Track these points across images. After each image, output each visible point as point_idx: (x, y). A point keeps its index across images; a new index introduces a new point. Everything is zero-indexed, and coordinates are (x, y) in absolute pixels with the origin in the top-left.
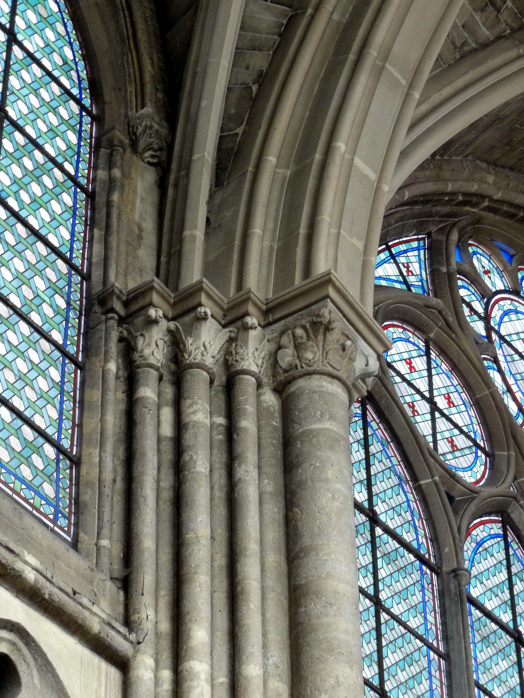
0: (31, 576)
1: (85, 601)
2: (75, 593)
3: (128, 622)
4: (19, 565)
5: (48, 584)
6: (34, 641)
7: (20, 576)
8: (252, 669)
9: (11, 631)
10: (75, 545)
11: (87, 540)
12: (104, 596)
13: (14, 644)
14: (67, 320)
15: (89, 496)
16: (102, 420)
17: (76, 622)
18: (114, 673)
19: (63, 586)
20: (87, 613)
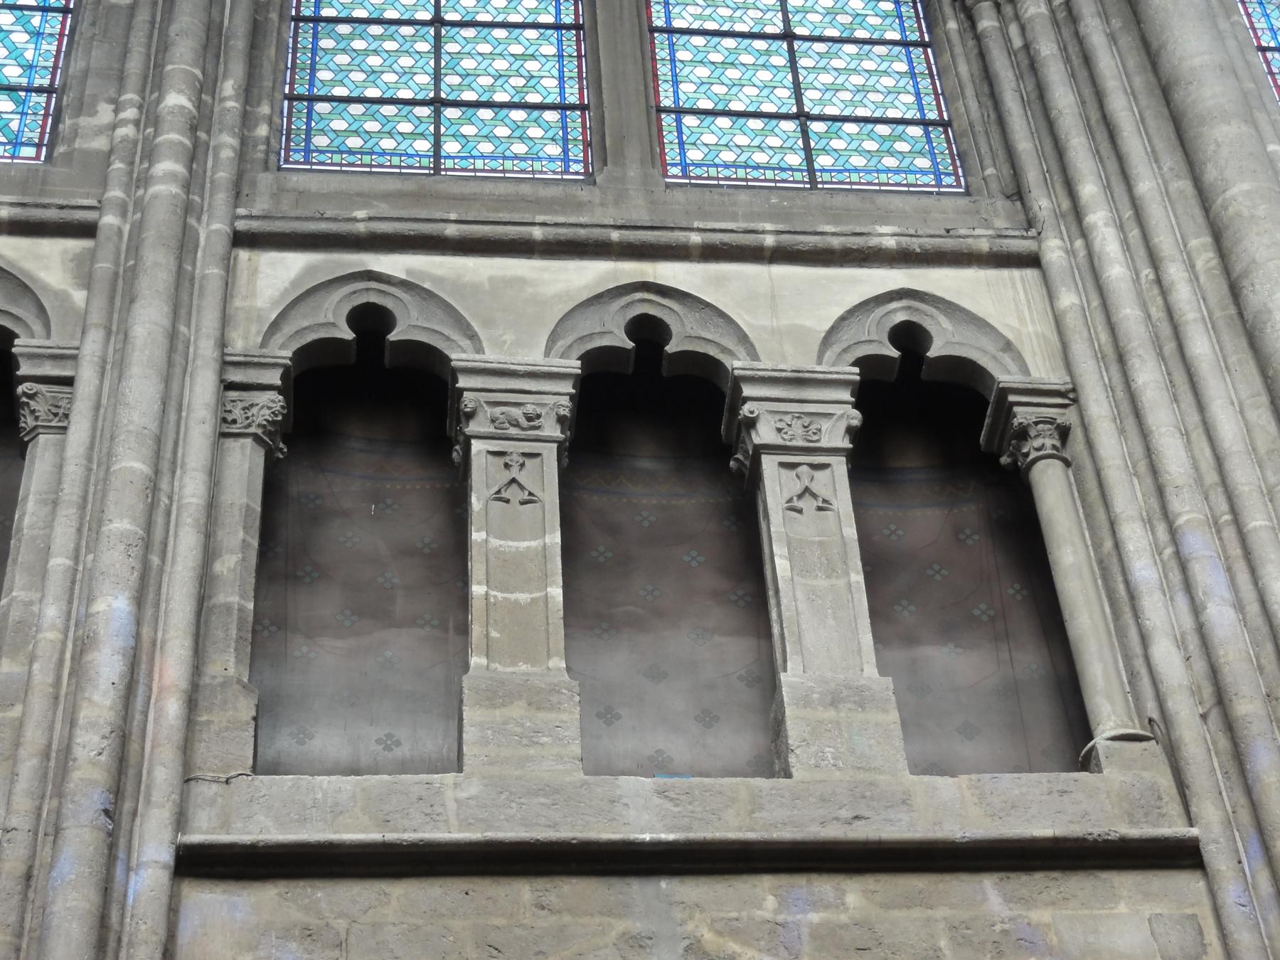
0: (890, 243)
1: (963, 232)
2: (948, 231)
4: (874, 241)
5: (914, 240)
6: (926, 294)
7: (880, 249)
9: (901, 299)
12: (997, 216)
13: (909, 308)
14: (900, 17)
16: (957, 74)
17: (963, 254)
19: (937, 233)
20: (970, 241)
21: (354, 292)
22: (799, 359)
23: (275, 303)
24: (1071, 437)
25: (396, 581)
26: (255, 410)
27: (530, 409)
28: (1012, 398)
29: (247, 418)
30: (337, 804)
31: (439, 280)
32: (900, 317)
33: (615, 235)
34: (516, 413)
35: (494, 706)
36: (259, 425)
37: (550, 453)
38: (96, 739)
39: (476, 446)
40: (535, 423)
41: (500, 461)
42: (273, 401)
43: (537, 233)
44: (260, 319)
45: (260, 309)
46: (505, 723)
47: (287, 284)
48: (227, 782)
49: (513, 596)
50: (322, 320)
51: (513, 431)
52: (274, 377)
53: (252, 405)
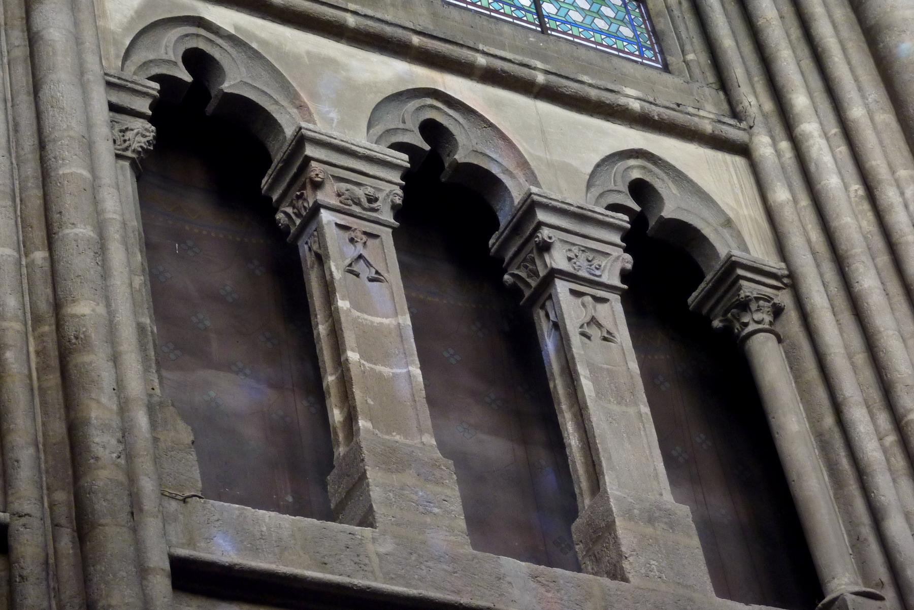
0: (636, 106)
1: (691, 110)
2: (678, 105)
3: (736, 114)
4: (622, 101)
5: (653, 107)
6: (660, 159)
7: (627, 109)
8: (856, 112)
9: (637, 157)
10: (666, 68)
11: (674, 60)
12: (707, 101)
13: (644, 168)
15: (663, 24)
17: (690, 131)
18: (739, 161)
19: (667, 104)
20: (696, 119)
21: (187, 35)
22: (574, 195)
23: (127, 29)
24: (784, 317)
25: (208, 323)
26: (129, 135)
27: (370, 191)
28: (740, 272)
29: (125, 141)
30: (280, 540)
31: (264, 43)
32: (636, 174)
33: (416, 40)
34: (360, 192)
35: (389, 470)
36: (134, 151)
37: (387, 235)
38: (114, 442)
39: (326, 216)
40: (375, 205)
41: (347, 235)
42: (146, 130)
43: (351, 21)
44: (116, 43)
45: (113, 33)
46: (402, 489)
47: (132, 13)
48: (184, 501)
49: (379, 368)
50: (165, 57)
51: (356, 209)
52: (143, 105)
53: (127, 129)
